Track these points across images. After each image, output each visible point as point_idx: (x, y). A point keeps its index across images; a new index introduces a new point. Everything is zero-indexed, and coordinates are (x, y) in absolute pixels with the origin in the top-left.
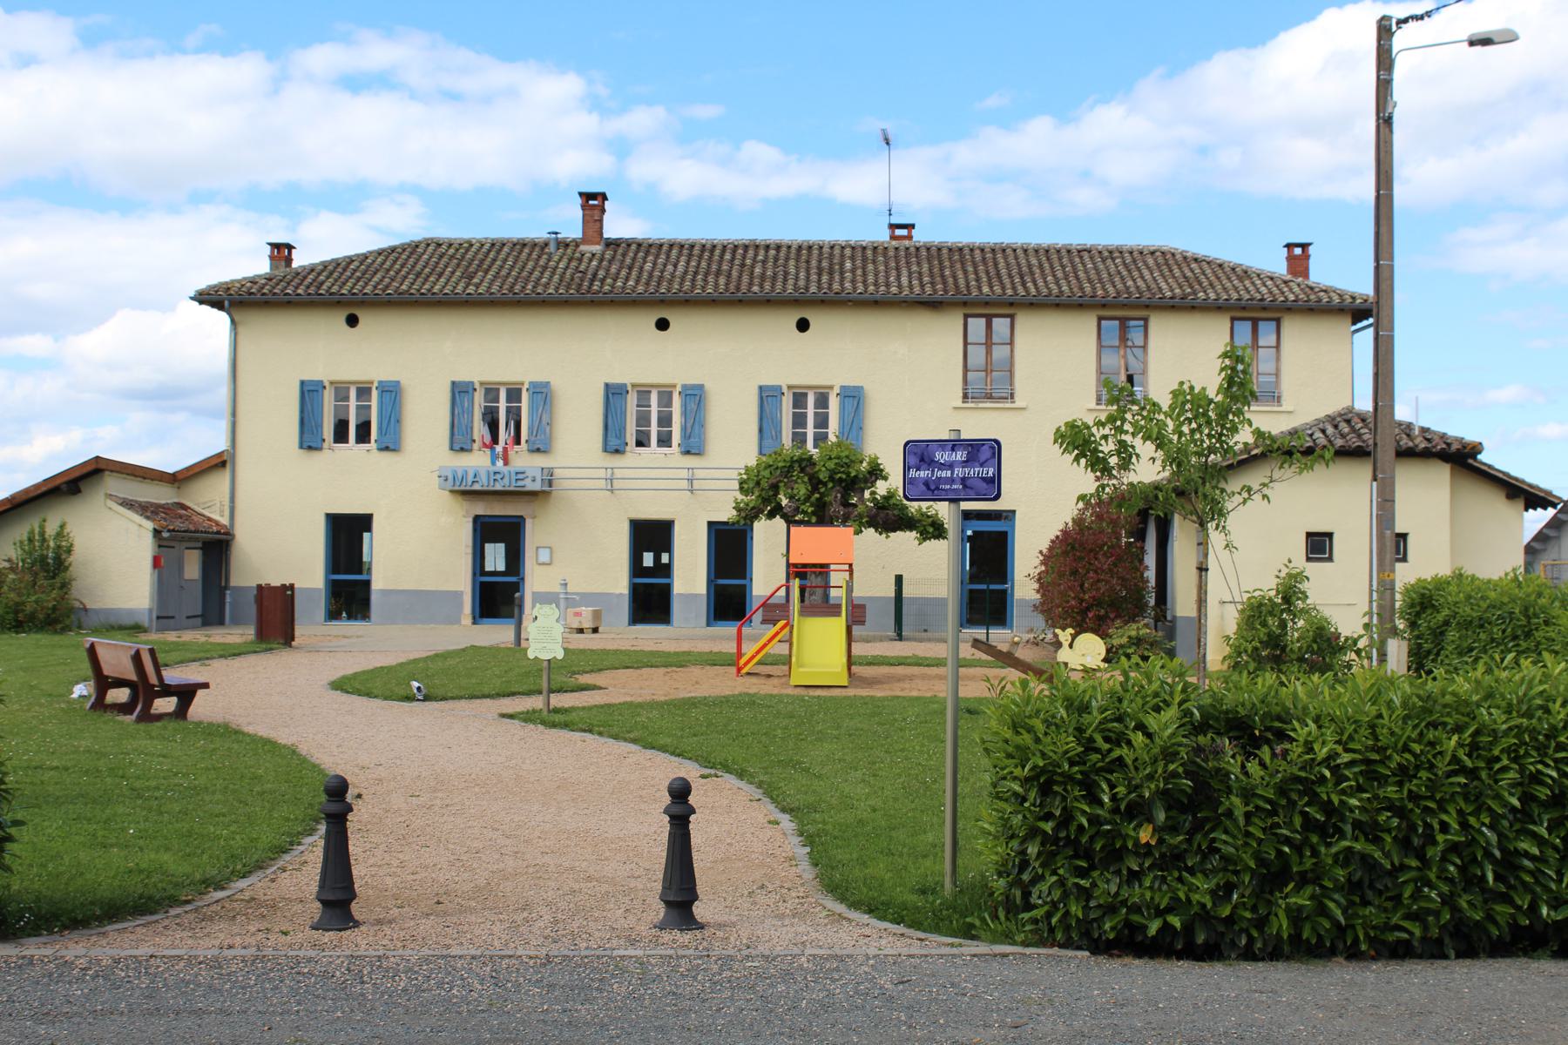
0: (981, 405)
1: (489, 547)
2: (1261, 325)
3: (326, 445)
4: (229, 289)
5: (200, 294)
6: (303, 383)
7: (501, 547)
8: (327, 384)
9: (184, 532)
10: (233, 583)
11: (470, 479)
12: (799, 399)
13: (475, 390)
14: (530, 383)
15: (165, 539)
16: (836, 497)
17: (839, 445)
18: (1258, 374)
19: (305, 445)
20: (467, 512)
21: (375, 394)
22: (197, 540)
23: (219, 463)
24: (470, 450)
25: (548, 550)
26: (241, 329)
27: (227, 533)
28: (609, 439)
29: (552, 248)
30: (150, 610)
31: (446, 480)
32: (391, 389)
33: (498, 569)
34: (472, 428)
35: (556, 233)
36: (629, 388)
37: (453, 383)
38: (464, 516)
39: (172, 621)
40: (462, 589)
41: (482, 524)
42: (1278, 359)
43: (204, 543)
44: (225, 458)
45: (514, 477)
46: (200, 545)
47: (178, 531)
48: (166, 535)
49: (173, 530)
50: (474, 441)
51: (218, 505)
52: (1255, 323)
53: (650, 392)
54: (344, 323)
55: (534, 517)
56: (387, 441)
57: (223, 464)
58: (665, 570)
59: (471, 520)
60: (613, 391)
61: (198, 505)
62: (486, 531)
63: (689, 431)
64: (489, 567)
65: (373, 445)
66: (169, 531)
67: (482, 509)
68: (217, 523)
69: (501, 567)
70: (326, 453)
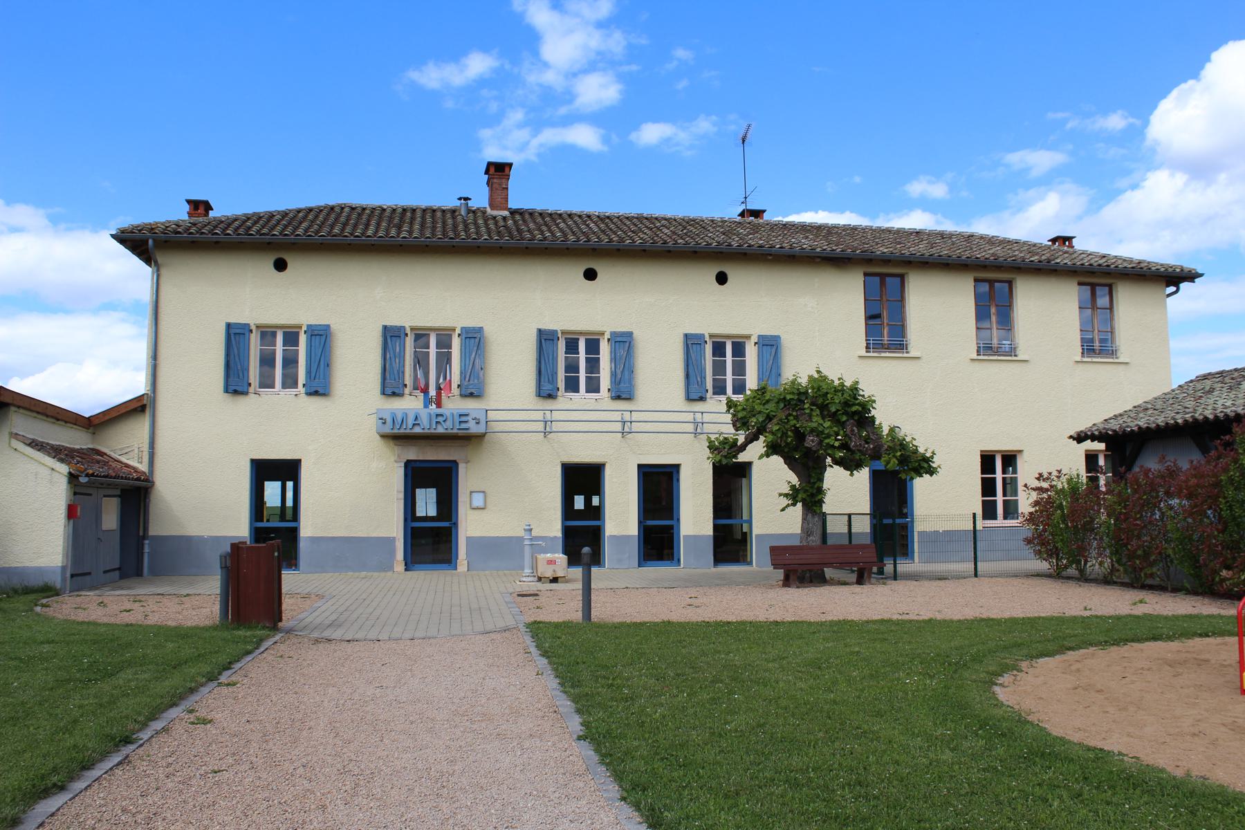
0: (883, 355)
1: (420, 493)
2: (1099, 291)
3: (251, 389)
4: (152, 229)
5: (123, 232)
6: (229, 326)
7: (432, 493)
8: (253, 328)
9: (104, 477)
10: (153, 531)
11: (411, 421)
12: (719, 349)
13: (407, 335)
14: (462, 328)
15: (82, 485)
16: (853, 431)
17: (762, 390)
18: (1099, 331)
19: (231, 388)
20: (398, 456)
21: (303, 339)
22: (115, 486)
23: (138, 408)
24: (401, 395)
25: (481, 495)
26: (163, 271)
27: (147, 480)
28: (542, 383)
29: (463, 213)
30: (64, 568)
31: (384, 423)
32: (321, 333)
33: (429, 514)
34: (403, 372)
35: (466, 199)
36: (560, 335)
37: (385, 327)
38: (396, 461)
39: (88, 578)
40: (395, 535)
41: (413, 469)
42: (1112, 319)
43: (122, 490)
44: (145, 402)
45: (457, 420)
46: (118, 492)
47: (97, 476)
48: (83, 480)
49: (93, 475)
50: (406, 385)
51: (136, 451)
52: (1093, 287)
53: (578, 339)
54: (273, 269)
55: (467, 462)
56: (316, 385)
57: (142, 409)
58: (596, 513)
59: (403, 465)
60: (545, 338)
61: (114, 451)
62: (417, 476)
63: (619, 376)
64: (420, 512)
65: (301, 389)
66: (87, 475)
67: (413, 454)
68: (136, 470)
69: (432, 512)
70: (252, 396)
